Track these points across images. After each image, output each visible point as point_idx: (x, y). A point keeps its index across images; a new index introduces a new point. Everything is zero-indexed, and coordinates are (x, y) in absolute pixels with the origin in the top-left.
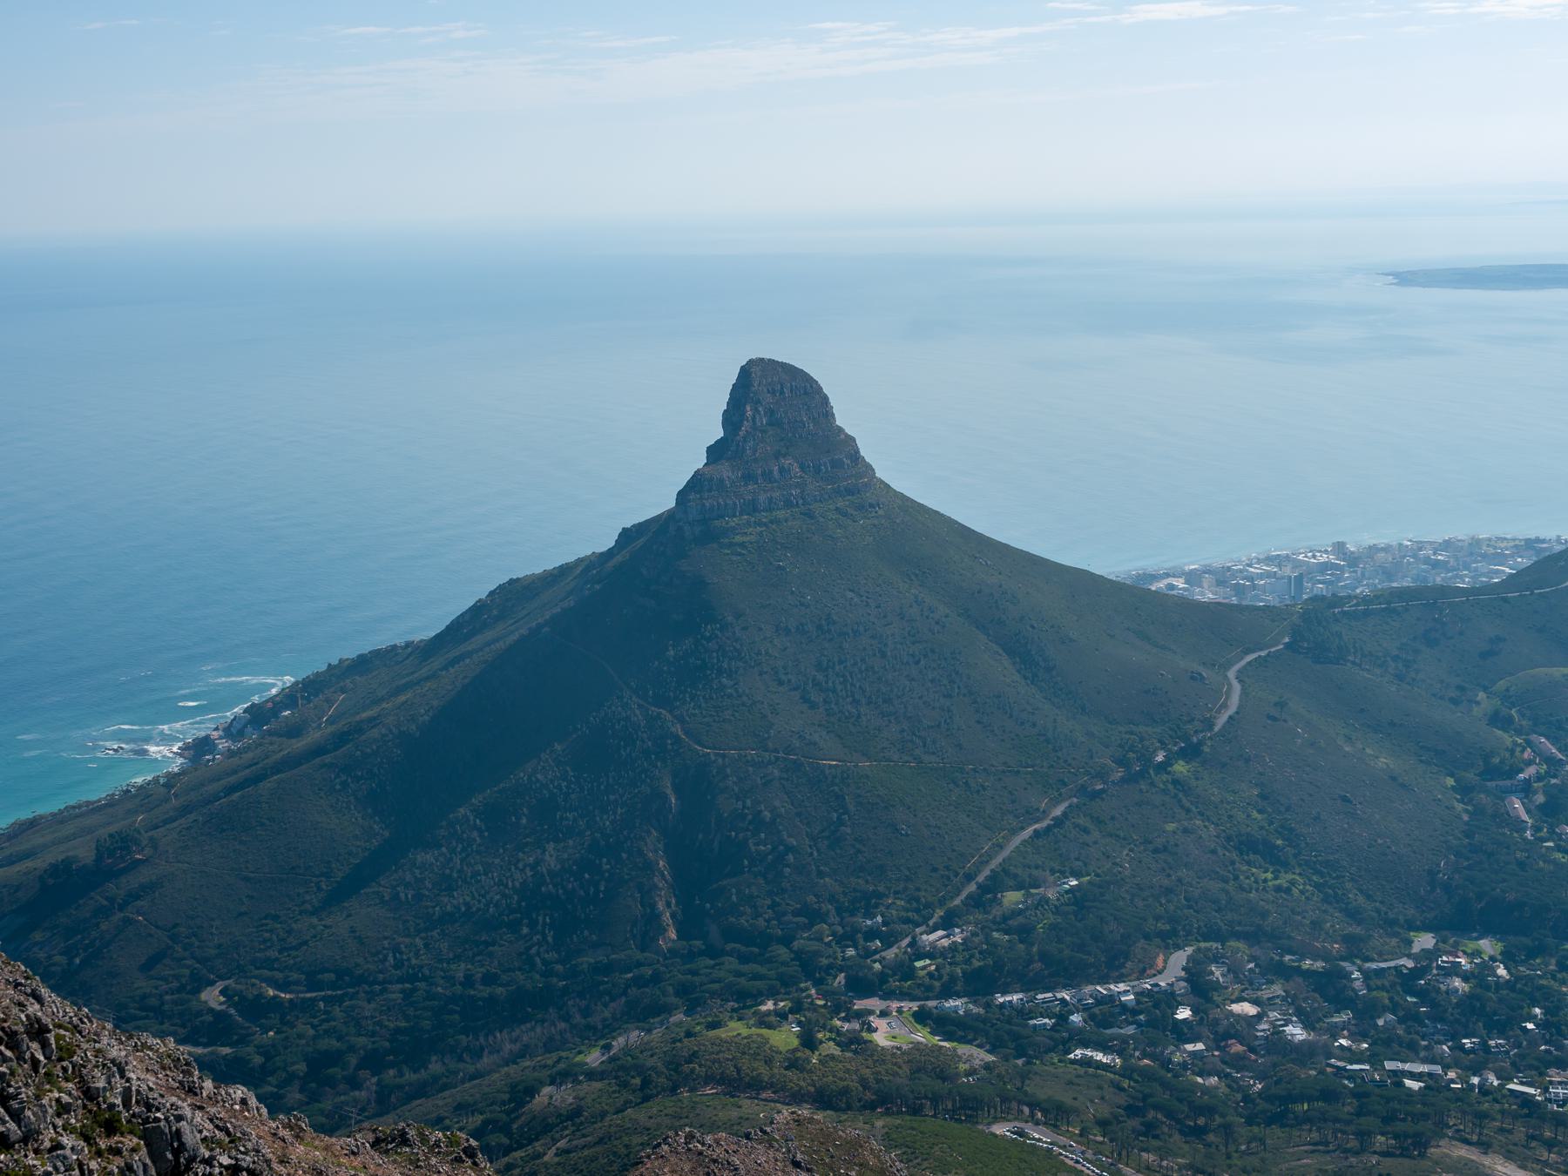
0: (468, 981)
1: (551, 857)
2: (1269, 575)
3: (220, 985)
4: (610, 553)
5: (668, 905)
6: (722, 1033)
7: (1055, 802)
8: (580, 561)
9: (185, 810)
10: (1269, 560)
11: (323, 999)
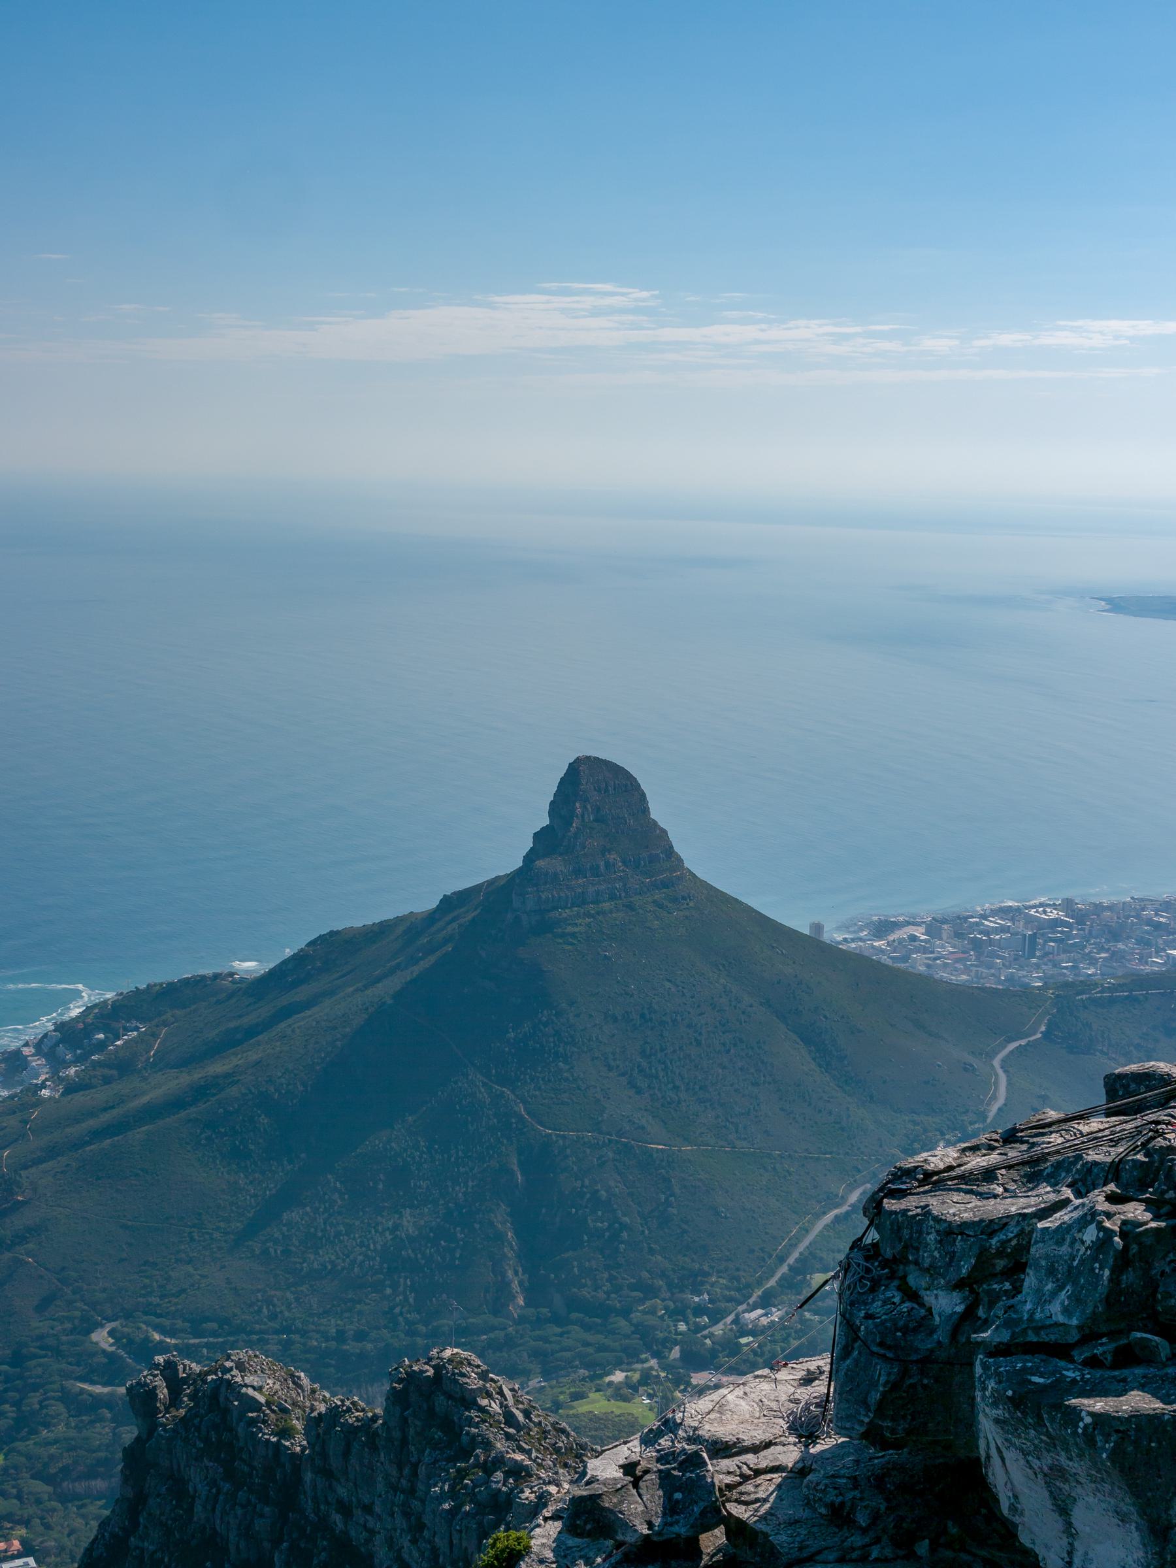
0: (341, 1336)
1: (409, 1222)
2: (1003, 929)
3: (109, 1326)
4: (432, 917)
5: (516, 1273)
6: (582, 1407)
7: (851, 1188)
8: (399, 920)
9: (52, 1152)
10: (1003, 912)
11: (207, 1345)
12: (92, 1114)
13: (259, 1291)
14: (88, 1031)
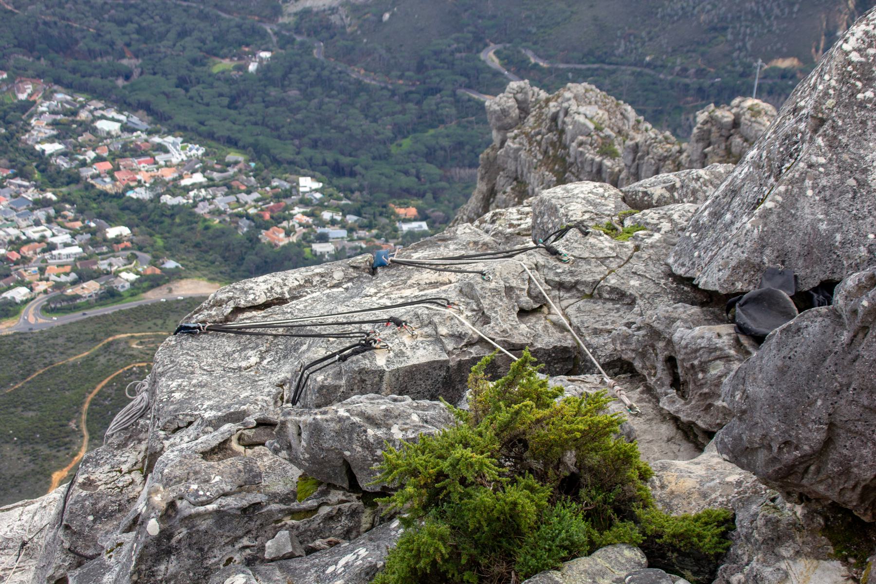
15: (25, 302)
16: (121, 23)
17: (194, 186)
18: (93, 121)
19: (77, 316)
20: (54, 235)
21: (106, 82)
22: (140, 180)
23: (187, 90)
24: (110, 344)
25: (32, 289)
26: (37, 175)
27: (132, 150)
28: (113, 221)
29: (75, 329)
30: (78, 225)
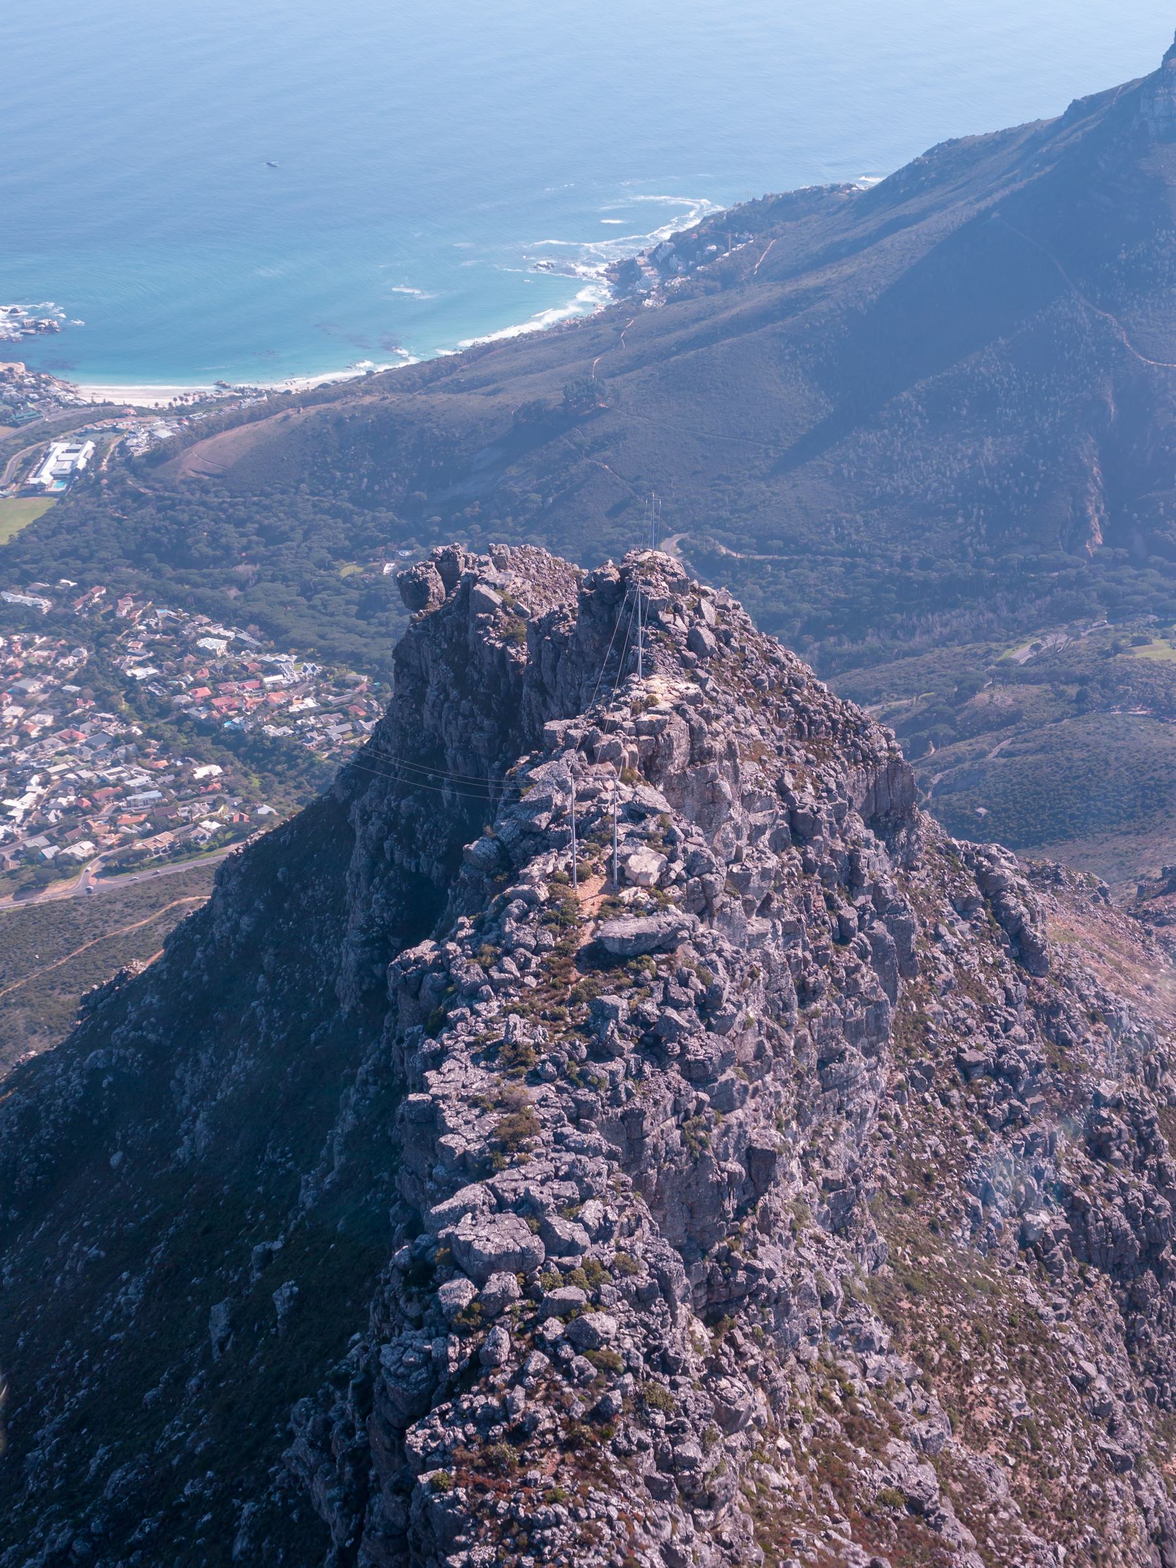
0: (906, 563)
3: (677, 537)
4: (1057, 125)
5: (1097, 510)
8: (1025, 127)
9: (640, 361)
11: (771, 562)
12: (683, 325)
13: (829, 511)
14: (701, 243)
15: (90, 858)
16: (240, 523)
17: (301, 714)
18: (195, 641)
19: (138, 877)
20: (132, 778)
21: (216, 594)
22: (238, 706)
23: (309, 599)
24: (173, 909)
25: (96, 843)
26: (124, 706)
27: (235, 672)
28: (203, 760)
29: (139, 891)
30: (163, 763)
